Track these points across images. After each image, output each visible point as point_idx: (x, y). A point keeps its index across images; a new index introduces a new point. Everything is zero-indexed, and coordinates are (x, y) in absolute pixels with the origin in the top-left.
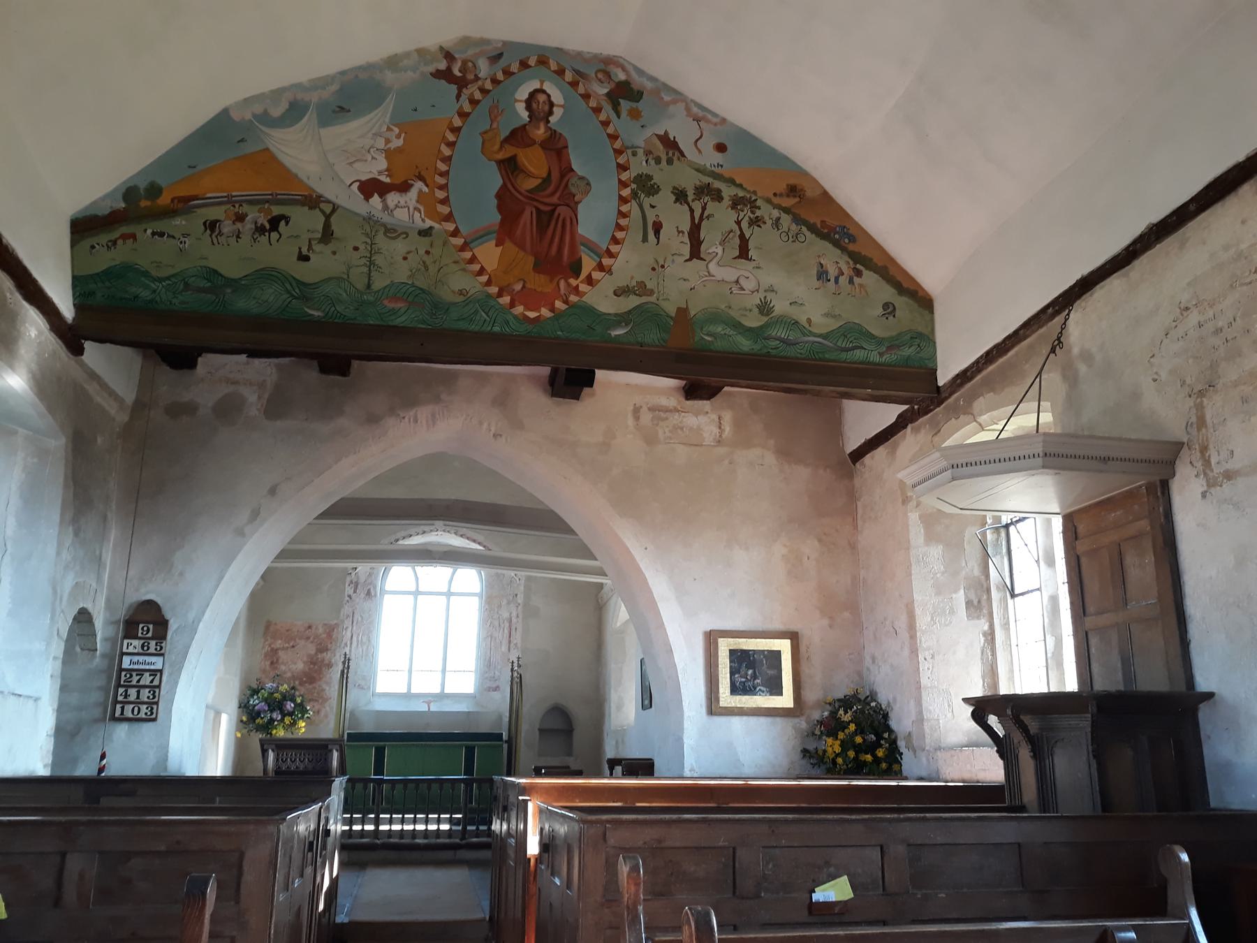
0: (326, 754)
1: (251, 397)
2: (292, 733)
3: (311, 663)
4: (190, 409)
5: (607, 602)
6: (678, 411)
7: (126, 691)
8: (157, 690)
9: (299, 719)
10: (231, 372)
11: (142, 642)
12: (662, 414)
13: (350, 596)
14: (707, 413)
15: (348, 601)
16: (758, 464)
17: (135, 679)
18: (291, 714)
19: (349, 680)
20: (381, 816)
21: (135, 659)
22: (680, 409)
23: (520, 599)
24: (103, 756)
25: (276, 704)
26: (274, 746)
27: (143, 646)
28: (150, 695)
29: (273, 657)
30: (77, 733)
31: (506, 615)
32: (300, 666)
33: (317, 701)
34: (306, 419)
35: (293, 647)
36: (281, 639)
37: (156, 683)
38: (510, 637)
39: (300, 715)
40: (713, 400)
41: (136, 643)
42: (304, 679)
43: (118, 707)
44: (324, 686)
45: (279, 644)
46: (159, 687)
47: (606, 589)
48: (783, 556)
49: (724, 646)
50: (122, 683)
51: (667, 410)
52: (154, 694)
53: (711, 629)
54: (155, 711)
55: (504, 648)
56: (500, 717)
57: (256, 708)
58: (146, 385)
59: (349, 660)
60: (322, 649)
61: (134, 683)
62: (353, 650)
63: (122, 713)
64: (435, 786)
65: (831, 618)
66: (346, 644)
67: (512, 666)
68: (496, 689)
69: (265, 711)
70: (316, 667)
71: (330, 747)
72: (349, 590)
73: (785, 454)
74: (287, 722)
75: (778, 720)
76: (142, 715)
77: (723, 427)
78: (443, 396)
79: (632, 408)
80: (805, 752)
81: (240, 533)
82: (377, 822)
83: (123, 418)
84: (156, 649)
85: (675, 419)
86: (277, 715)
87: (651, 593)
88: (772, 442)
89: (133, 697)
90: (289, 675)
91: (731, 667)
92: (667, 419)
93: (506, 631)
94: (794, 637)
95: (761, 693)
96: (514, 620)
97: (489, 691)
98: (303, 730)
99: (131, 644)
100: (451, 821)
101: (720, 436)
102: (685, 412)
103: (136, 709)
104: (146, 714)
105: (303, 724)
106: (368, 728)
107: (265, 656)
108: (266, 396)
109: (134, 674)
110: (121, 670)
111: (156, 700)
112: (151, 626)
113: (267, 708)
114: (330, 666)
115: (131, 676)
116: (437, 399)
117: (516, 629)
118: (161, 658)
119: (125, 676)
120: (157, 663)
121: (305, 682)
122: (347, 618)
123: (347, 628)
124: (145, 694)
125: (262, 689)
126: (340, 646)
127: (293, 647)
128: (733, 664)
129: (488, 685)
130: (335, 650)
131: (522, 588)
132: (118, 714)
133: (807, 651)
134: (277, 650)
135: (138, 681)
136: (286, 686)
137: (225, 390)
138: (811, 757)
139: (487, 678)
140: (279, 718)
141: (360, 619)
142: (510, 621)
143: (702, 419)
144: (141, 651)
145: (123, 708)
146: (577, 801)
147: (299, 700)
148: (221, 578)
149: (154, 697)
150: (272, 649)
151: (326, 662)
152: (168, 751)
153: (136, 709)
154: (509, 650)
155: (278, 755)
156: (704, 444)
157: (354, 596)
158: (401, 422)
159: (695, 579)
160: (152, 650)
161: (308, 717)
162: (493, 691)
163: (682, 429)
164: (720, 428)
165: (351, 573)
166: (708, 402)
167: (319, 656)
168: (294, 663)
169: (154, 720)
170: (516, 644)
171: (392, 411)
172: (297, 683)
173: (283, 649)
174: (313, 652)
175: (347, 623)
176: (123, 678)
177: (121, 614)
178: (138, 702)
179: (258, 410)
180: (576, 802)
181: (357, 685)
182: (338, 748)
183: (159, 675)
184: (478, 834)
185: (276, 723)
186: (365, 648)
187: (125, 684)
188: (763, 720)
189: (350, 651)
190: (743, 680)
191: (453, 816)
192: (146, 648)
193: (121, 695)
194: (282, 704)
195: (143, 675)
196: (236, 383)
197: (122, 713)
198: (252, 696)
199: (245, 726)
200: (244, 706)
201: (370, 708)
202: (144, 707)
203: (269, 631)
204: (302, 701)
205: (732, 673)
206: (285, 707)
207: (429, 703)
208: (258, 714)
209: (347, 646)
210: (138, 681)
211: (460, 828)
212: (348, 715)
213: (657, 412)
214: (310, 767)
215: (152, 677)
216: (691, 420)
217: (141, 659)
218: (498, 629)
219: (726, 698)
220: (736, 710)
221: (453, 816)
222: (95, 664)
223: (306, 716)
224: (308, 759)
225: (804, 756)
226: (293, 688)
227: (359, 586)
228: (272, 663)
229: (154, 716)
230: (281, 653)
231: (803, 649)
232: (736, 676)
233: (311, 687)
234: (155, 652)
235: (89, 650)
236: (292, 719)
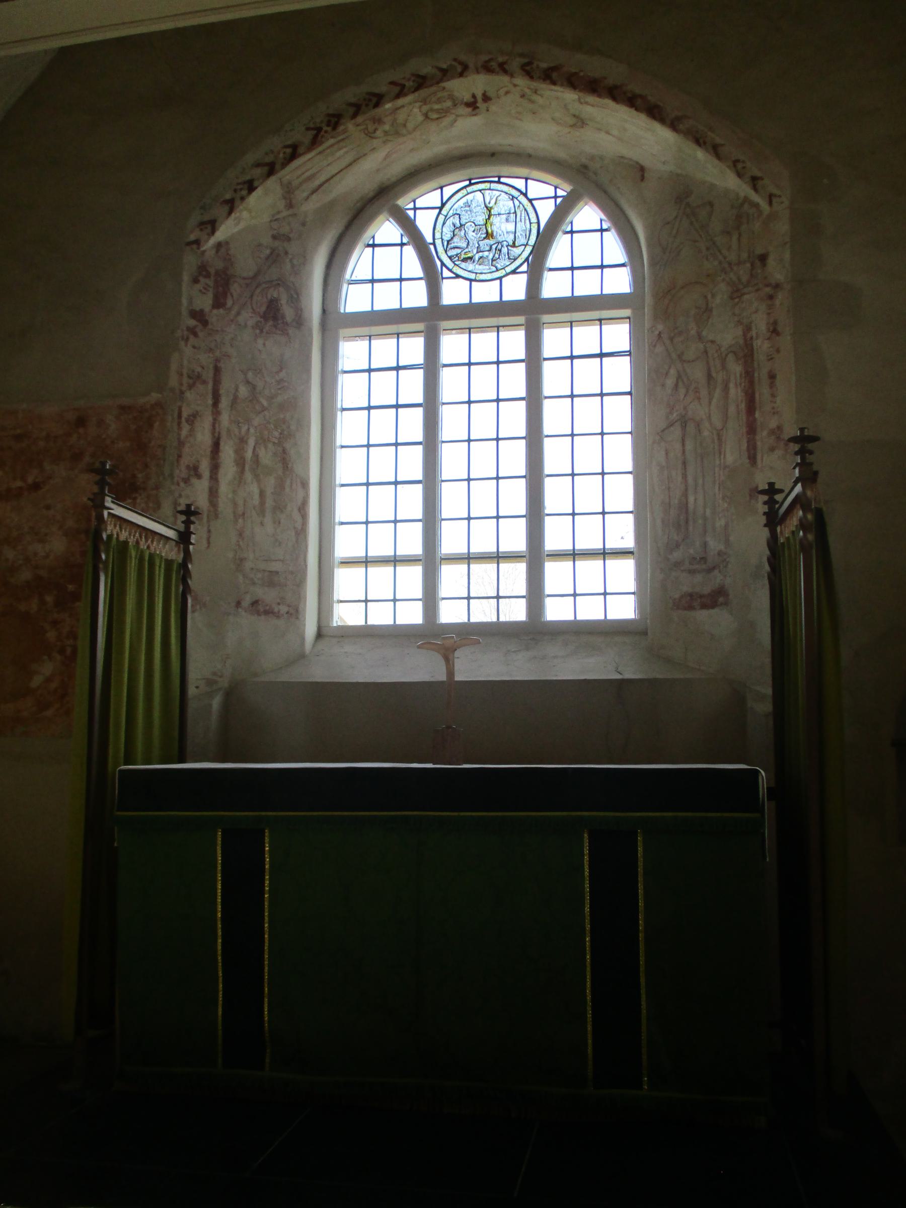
15: (193, 331)
23: (777, 271)
32: (58, 545)
35: (36, 486)
38: (751, 408)
55: (733, 454)
62: (224, 488)
66: (195, 470)
90: (26, 575)
93: (736, 393)
96: (762, 346)
97: (691, 608)
117: (772, 377)
122: (191, 387)
123: (193, 418)
126: (171, 476)
127: (36, 486)
129: (686, 589)
130: (157, 488)
131: (783, 227)
139: (677, 564)
141: (243, 391)
154: (753, 459)
157: (215, 316)
162: (704, 606)
165: (197, 242)
172: (49, 599)
181: (246, 603)
186: (270, 483)
189: (213, 493)
201: (285, 677)
207: (448, 654)
209: (199, 476)
218: (704, 392)
227: (235, 289)
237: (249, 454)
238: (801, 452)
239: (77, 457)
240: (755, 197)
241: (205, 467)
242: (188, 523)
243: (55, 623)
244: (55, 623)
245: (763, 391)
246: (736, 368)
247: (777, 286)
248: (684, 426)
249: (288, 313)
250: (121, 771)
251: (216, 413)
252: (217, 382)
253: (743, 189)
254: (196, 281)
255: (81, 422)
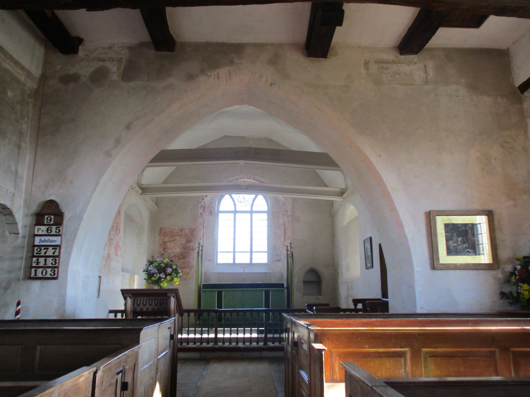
0: (167, 300)
1: (113, 68)
2: (172, 285)
3: (184, 248)
4: (75, 78)
5: (337, 213)
6: (395, 63)
7: (38, 260)
8: (57, 259)
9: (175, 277)
10: (100, 54)
11: (47, 227)
12: (385, 65)
13: (201, 214)
14: (416, 63)
16: (455, 96)
17: (43, 251)
18: (170, 274)
19: (203, 257)
20: (218, 329)
21: (43, 238)
22: (397, 61)
23: (289, 213)
24: (19, 304)
25: (162, 269)
26: (130, 295)
27: (47, 230)
28: (53, 262)
29: (164, 245)
30: (8, 289)
31: (282, 222)
32: (178, 250)
33: (187, 268)
34: (148, 80)
35: (174, 240)
36: (168, 236)
37: (57, 254)
38: (285, 233)
39: (175, 275)
40: (419, 54)
41: (44, 228)
42: (181, 257)
43: (33, 270)
44: (191, 260)
45: (167, 239)
46: (58, 256)
47: (336, 205)
48: (477, 158)
49: (441, 222)
50: (35, 254)
51: (387, 62)
52: (55, 262)
53: (430, 210)
54: (56, 272)
55: (282, 239)
56: (282, 276)
57: (152, 272)
58: (46, 64)
59: (202, 246)
60: (189, 241)
61: (43, 254)
63: (35, 275)
64: (248, 314)
65: (514, 200)
67: (287, 248)
68: (279, 260)
69: (156, 273)
70: (186, 250)
71: (168, 295)
72: (201, 211)
73: (473, 87)
74: (169, 279)
75: (481, 272)
76: (48, 275)
77: (427, 72)
78: (236, 61)
79: (363, 62)
80: (503, 295)
81: (108, 154)
82: (216, 333)
83: (31, 85)
84: (56, 232)
85: (394, 68)
86: (162, 275)
87: (385, 186)
88: (463, 81)
89: (42, 264)
90: (172, 255)
91: (446, 236)
92: (387, 68)
93: (283, 230)
94: (490, 214)
95: (469, 254)
96: (286, 224)
97: (276, 262)
98: (178, 283)
99: (40, 229)
100: (259, 332)
101: (427, 78)
102: (400, 63)
103: (44, 271)
104: (51, 274)
105: (178, 280)
106: (214, 281)
107: (161, 246)
108: (123, 67)
109: (42, 248)
110: (35, 246)
111: (57, 265)
112: (52, 217)
113: (157, 272)
114: (193, 250)
115: (41, 250)
116: (232, 63)
117: (288, 229)
118: (59, 238)
119: (37, 250)
120: (57, 240)
121: (181, 258)
123: (200, 231)
124: (50, 261)
125: (155, 261)
127: (174, 240)
128: (447, 234)
130: (195, 241)
132: (33, 275)
133: (499, 224)
134: (166, 242)
135: (45, 253)
136: (167, 260)
137: (96, 65)
138: (508, 298)
140: (164, 276)
142: (285, 225)
143: (413, 67)
144: (47, 233)
145: (36, 271)
146: (367, 346)
147: (174, 267)
148: (97, 184)
149: (56, 263)
150: (164, 242)
151: (191, 248)
152: (65, 299)
153: (44, 271)
154: (285, 240)
155: (134, 301)
156: (415, 84)
157: (203, 214)
158: (209, 78)
159: (416, 176)
160: (53, 233)
161: (180, 276)
163: (399, 74)
164: (426, 73)
166: (416, 56)
167: (187, 245)
168: (175, 249)
169: (56, 278)
170: (288, 237)
171: (203, 71)
172: (177, 259)
173: (169, 241)
174: (184, 242)
175: (201, 227)
176: (36, 252)
177: (34, 208)
178: (45, 267)
179: (117, 76)
180: (364, 348)
181: (207, 260)
182: (175, 295)
183: (58, 248)
184: (273, 340)
185: (162, 279)
187: (37, 255)
188: (470, 272)
190: (455, 244)
191: (259, 329)
192: (49, 231)
193: (34, 262)
194: (165, 270)
195: (48, 249)
196: (103, 60)
197: (35, 275)
198: (150, 265)
199: (147, 281)
200: (147, 271)
202: (49, 270)
203: (162, 232)
204: (177, 267)
205: (447, 240)
206: (167, 271)
207: (244, 268)
208: (153, 274)
209: (201, 240)
210: (45, 253)
211: (263, 336)
212: (203, 275)
213: (381, 63)
214: (156, 308)
215: (54, 250)
216: (405, 68)
217: (47, 238)
219: (444, 258)
220: (451, 266)
221: (259, 329)
222: (18, 244)
223: (179, 275)
224: (155, 303)
225: (502, 298)
226: (171, 261)
227: (206, 209)
228: (164, 249)
229: (55, 276)
230: (168, 244)
231: (496, 223)
232: (450, 242)
233: (184, 261)
234: (55, 234)
235: (14, 233)
236: (171, 277)
237: (208, 236)
238: (290, 245)
239: (181, 236)
240: (286, 201)
241: (202, 238)
242: (202, 248)
243: (178, 263)
244: (178, 263)
245: (287, 231)
246: (283, 227)
247: (289, 216)
248: (275, 234)
249: (213, 212)
250: (203, 284)
251: (203, 229)
252: (204, 224)
253: (285, 200)
254: (201, 208)
255: (182, 230)
